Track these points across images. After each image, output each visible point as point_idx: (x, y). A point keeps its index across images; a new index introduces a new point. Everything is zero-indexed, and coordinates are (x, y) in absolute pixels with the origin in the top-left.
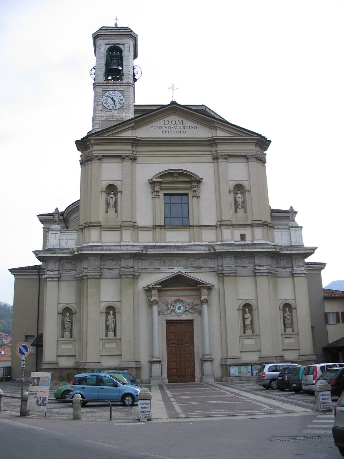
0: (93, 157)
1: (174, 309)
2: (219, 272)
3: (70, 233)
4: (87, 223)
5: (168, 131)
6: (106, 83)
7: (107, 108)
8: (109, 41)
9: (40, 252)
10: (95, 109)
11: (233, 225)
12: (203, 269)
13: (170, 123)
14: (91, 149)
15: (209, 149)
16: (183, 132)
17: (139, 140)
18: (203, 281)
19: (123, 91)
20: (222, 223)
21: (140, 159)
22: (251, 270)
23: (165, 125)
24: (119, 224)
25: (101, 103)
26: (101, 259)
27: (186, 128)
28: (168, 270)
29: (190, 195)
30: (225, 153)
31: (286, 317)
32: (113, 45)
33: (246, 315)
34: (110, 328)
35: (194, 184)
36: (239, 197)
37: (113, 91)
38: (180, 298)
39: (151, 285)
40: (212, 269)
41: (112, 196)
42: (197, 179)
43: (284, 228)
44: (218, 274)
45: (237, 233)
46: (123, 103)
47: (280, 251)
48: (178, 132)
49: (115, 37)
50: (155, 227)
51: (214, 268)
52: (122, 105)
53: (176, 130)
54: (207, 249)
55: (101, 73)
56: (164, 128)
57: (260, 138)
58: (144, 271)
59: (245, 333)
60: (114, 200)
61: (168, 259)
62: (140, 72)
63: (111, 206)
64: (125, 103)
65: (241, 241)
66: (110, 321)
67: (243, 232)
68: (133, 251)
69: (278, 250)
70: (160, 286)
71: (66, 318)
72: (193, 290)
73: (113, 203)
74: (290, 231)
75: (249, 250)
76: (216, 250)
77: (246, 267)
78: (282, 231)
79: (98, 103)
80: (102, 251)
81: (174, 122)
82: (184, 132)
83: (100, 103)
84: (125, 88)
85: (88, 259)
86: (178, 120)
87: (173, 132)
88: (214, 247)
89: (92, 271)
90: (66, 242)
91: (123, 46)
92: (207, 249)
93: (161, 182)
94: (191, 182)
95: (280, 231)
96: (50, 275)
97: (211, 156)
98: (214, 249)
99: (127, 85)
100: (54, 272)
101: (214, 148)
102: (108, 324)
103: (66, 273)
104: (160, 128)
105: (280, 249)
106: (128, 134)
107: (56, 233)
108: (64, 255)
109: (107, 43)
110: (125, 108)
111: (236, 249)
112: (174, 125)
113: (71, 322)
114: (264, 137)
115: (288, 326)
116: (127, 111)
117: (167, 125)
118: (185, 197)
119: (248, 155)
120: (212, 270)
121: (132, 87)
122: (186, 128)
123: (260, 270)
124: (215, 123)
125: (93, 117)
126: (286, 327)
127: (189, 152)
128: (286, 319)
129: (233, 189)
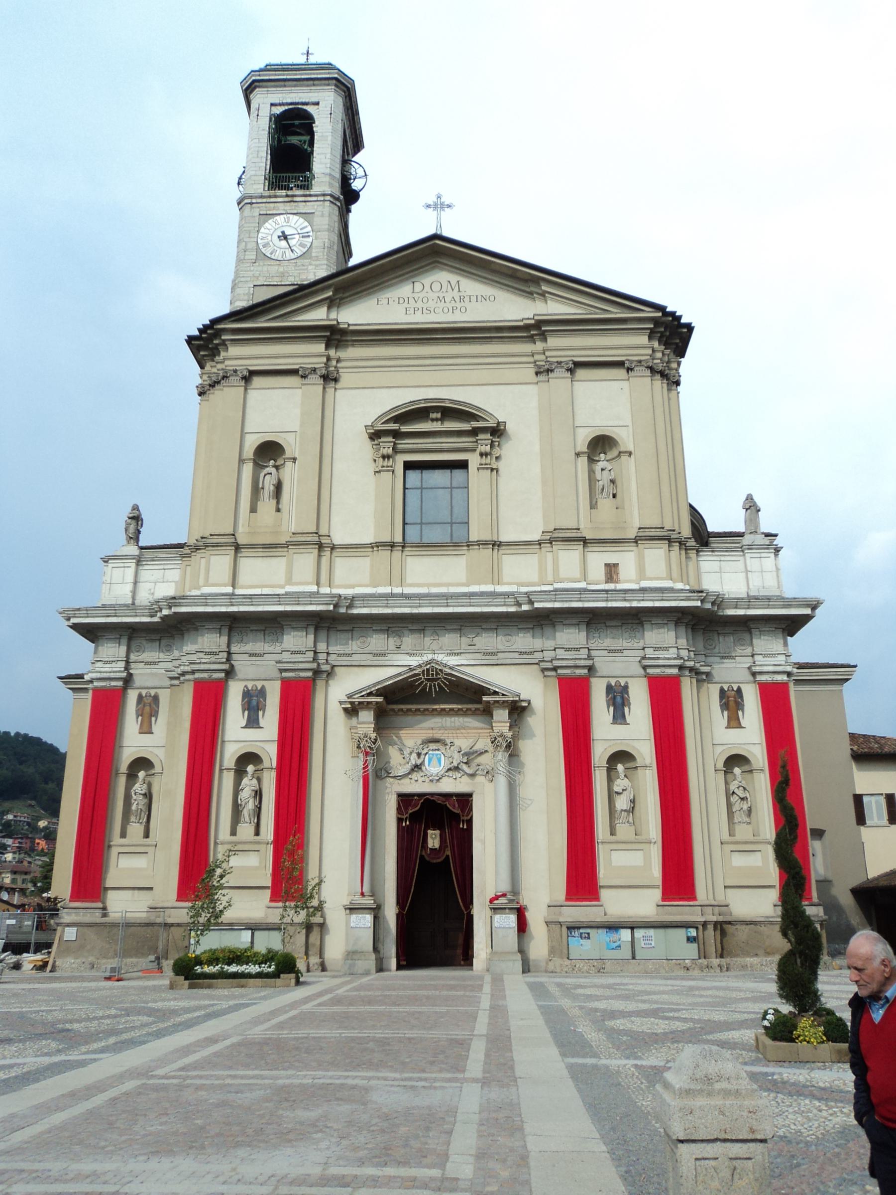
0: (225, 375)
1: (419, 762)
2: (544, 665)
3: (162, 567)
4: (202, 538)
5: (421, 309)
6: (270, 197)
7: (269, 256)
8: (280, 95)
9: (76, 612)
10: (239, 261)
11: (585, 542)
12: (500, 655)
13: (427, 288)
14: (223, 354)
15: (527, 348)
16: (459, 308)
17: (344, 332)
18: (496, 687)
19: (311, 215)
20: (556, 535)
21: (346, 378)
22: (632, 659)
23: (414, 295)
24: (283, 540)
25: (255, 245)
26: (230, 630)
27: (467, 299)
28: (407, 657)
29: (473, 466)
30: (569, 356)
31: (733, 793)
32: (291, 107)
33: (618, 782)
34: (245, 813)
35: (481, 436)
36: (602, 470)
37: (285, 216)
38: (438, 735)
39: (355, 697)
40: (525, 656)
41: (273, 470)
42: (492, 423)
43: (727, 551)
44: (543, 670)
45: (598, 559)
46: (309, 245)
47: (716, 608)
48: (446, 310)
49: (295, 86)
50: (378, 546)
51: (531, 653)
52: (306, 249)
53: (442, 304)
54: (511, 600)
55: (259, 173)
56: (411, 300)
57: (660, 314)
58: (344, 661)
59: (613, 833)
60: (275, 481)
61: (410, 630)
62: (360, 172)
63: (266, 495)
64: (314, 245)
65: (607, 582)
66: (246, 794)
67: (612, 558)
68: (312, 606)
69: (708, 606)
70: (380, 699)
71: (137, 786)
72: (474, 713)
73: (272, 488)
74: (745, 559)
75: (627, 604)
76: (535, 604)
77: (621, 651)
78: (722, 558)
79: (246, 246)
80: (232, 605)
81: (436, 287)
82: (463, 310)
83: (251, 245)
84: (316, 207)
85: (196, 629)
86: (449, 282)
87: (432, 311)
88: (528, 597)
89: (205, 661)
90: (150, 590)
91: (317, 107)
92: (511, 600)
93: (396, 434)
94: (474, 432)
95: (718, 558)
96: (100, 672)
97: (532, 365)
98: (531, 602)
99: (322, 198)
100: (114, 665)
101: (539, 346)
102: (239, 802)
103: (147, 666)
104: (401, 301)
105: (713, 603)
106: (319, 316)
107: (126, 565)
108: (137, 620)
109: (277, 101)
110: (314, 254)
111: (589, 601)
112: (437, 294)
113: (149, 796)
114: (673, 314)
115: (740, 820)
116: (318, 262)
117: (419, 295)
118: (458, 474)
119: (628, 360)
120: (526, 659)
121: (335, 204)
122: (467, 299)
123: (658, 658)
124: (542, 284)
125: (234, 281)
126: (736, 820)
127: (477, 357)
128: (734, 799)
129: (588, 448)
